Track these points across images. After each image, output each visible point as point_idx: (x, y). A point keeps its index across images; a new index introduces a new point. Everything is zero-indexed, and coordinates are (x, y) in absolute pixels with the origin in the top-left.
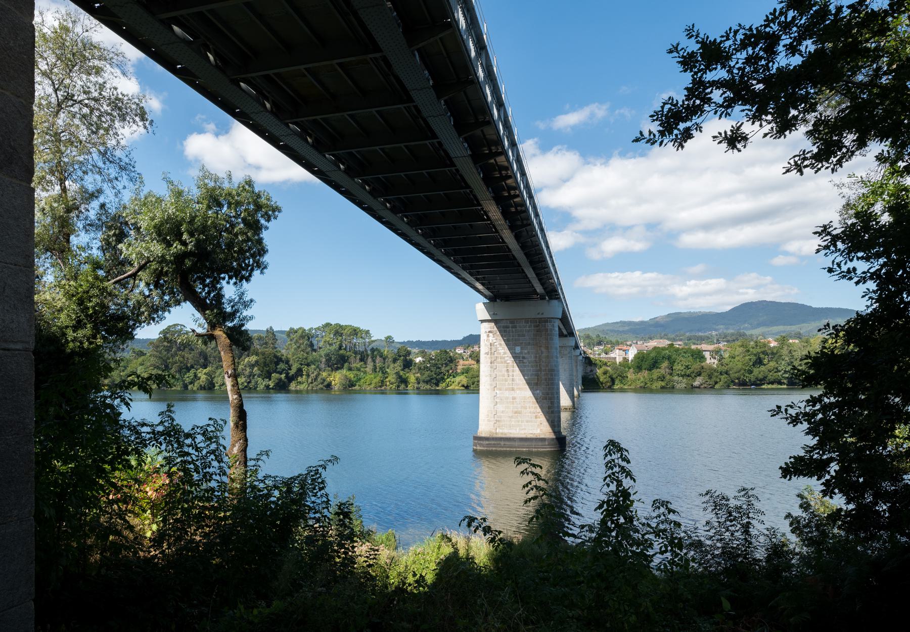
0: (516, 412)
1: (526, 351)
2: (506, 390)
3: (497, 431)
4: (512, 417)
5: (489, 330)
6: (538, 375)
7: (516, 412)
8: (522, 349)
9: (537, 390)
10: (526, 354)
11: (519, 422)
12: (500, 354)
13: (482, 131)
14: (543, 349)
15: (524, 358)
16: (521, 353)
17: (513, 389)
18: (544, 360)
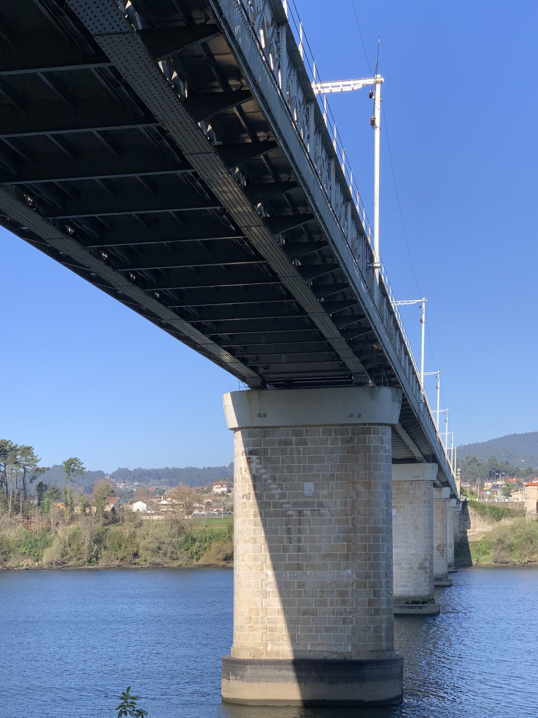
0: (305, 613)
1: (325, 492)
2: (285, 569)
3: (269, 648)
5: (251, 448)
6: (348, 540)
7: (305, 613)
8: (316, 486)
9: (347, 568)
10: (325, 497)
11: (311, 630)
12: (273, 496)
13: (205, 46)
14: (360, 488)
15: (321, 505)
16: (316, 495)
17: (299, 567)
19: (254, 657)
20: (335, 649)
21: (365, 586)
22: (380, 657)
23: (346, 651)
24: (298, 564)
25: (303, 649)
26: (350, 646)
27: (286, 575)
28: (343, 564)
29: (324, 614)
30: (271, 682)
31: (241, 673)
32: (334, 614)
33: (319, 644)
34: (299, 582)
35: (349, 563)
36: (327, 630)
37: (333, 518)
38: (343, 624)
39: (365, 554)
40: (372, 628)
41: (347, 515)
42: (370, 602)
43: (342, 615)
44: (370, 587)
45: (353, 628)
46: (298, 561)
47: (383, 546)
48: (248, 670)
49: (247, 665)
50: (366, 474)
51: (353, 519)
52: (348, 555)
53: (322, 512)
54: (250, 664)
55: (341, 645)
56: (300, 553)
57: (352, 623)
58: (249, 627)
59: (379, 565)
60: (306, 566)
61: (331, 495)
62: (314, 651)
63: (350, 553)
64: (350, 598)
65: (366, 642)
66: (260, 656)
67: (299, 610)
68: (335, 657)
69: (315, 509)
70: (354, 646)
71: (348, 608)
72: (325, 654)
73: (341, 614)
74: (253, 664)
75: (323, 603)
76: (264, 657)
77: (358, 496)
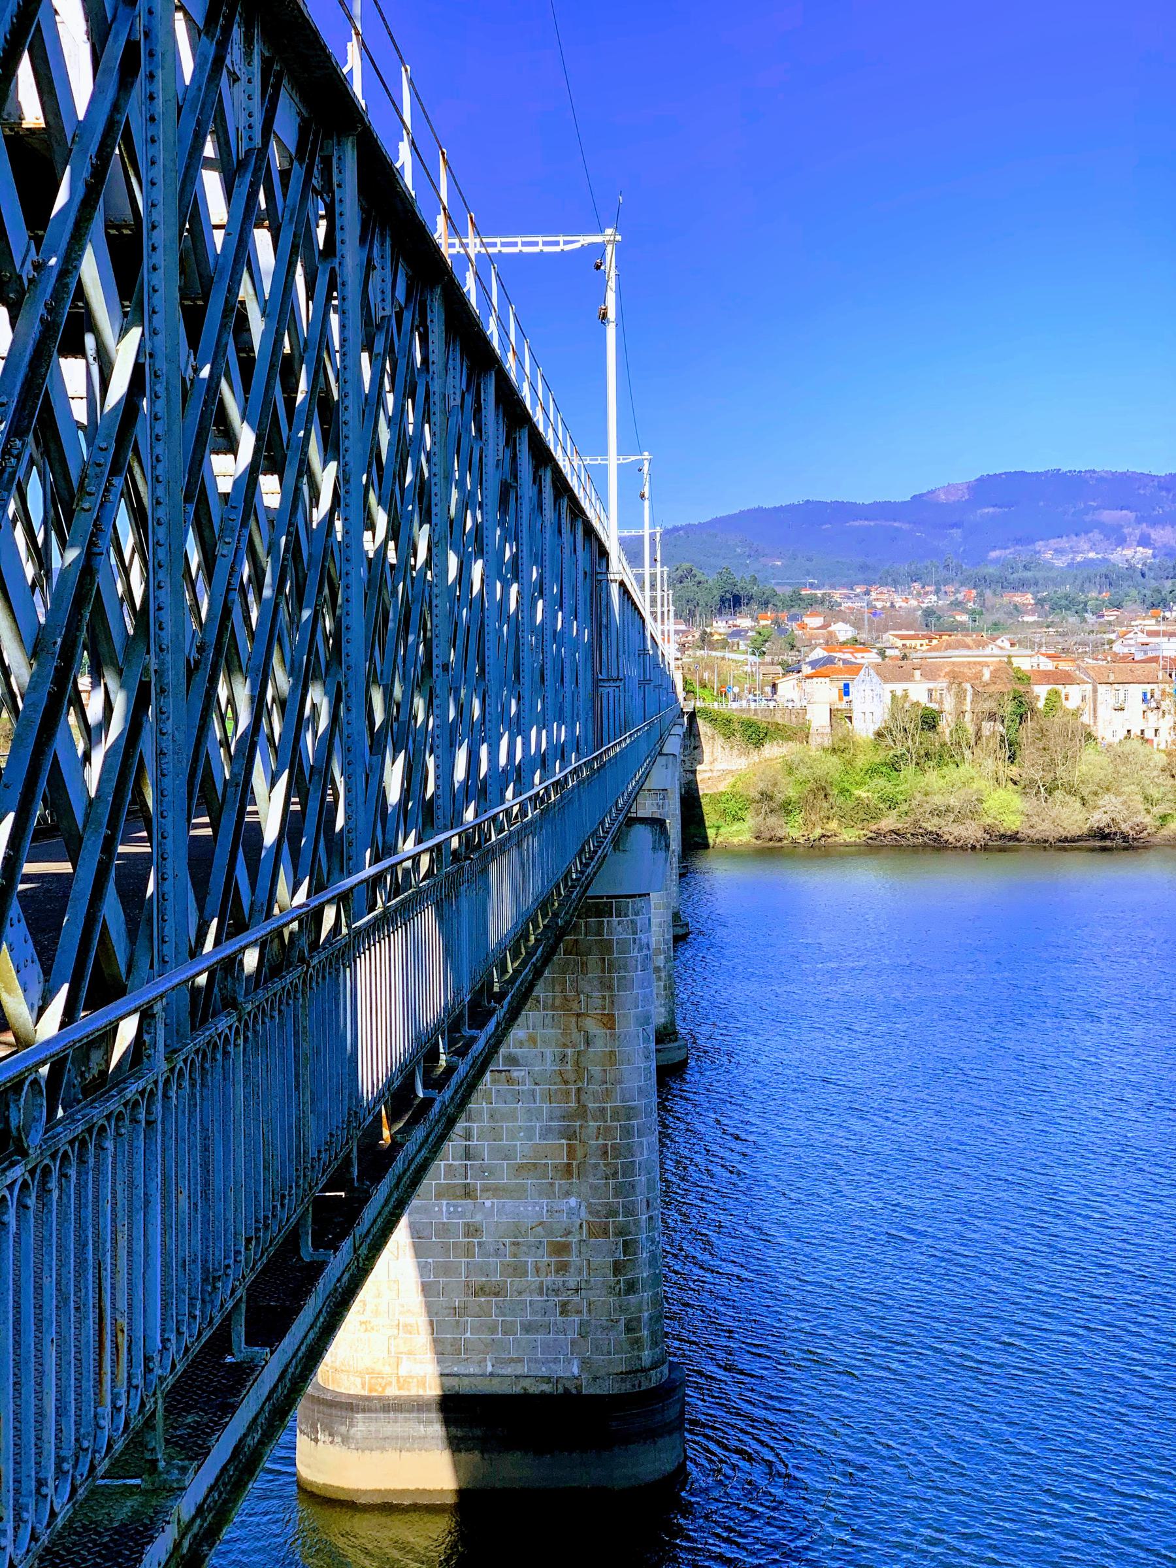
0: (481, 1291)
2: (439, 1196)
4: (463, 1310)
6: (571, 1135)
7: (481, 1291)
9: (568, 1194)
11: (493, 1330)
17: (468, 1192)
18: (596, 1070)
19: (371, 1390)
20: (544, 1371)
21: (606, 1233)
22: (640, 1386)
23: (568, 1374)
24: (466, 1186)
25: (477, 1371)
26: (576, 1362)
27: (441, 1210)
28: (560, 1185)
29: (520, 1293)
30: (408, 1450)
31: (343, 1429)
32: (541, 1294)
33: (512, 1360)
34: (467, 1225)
35: (571, 1184)
36: (528, 1328)
37: (537, 1087)
38: (561, 1313)
39: (606, 1165)
40: (623, 1322)
41: (566, 1083)
42: (618, 1268)
43: (557, 1295)
44: (616, 1235)
45: (581, 1324)
46: (466, 1178)
47: (641, 1143)
48: (360, 1424)
49: (358, 1412)
50: (604, 997)
51: (579, 1090)
52: (569, 1165)
53: (515, 1074)
54: (364, 1411)
55: (556, 1361)
56: (468, 1163)
57: (579, 1312)
58: (361, 1323)
59: (633, 1186)
60: (482, 1191)
61: (532, 1040)
62: (498, 1376)
63: (575, 1163)
64: (573, 1258)
65: (609, 1353)
66: (384, 1389)
67: (467, 1284)
68: (546, 1388)
69: (501, 1068)
70: (585, 1363)
71: (572, 1281)
72: (526, 1383)
73: (557, 1292)
74: (370, 1410)
75: (518, 1270)
76: (392, 1391)
77: (588, 1044)
